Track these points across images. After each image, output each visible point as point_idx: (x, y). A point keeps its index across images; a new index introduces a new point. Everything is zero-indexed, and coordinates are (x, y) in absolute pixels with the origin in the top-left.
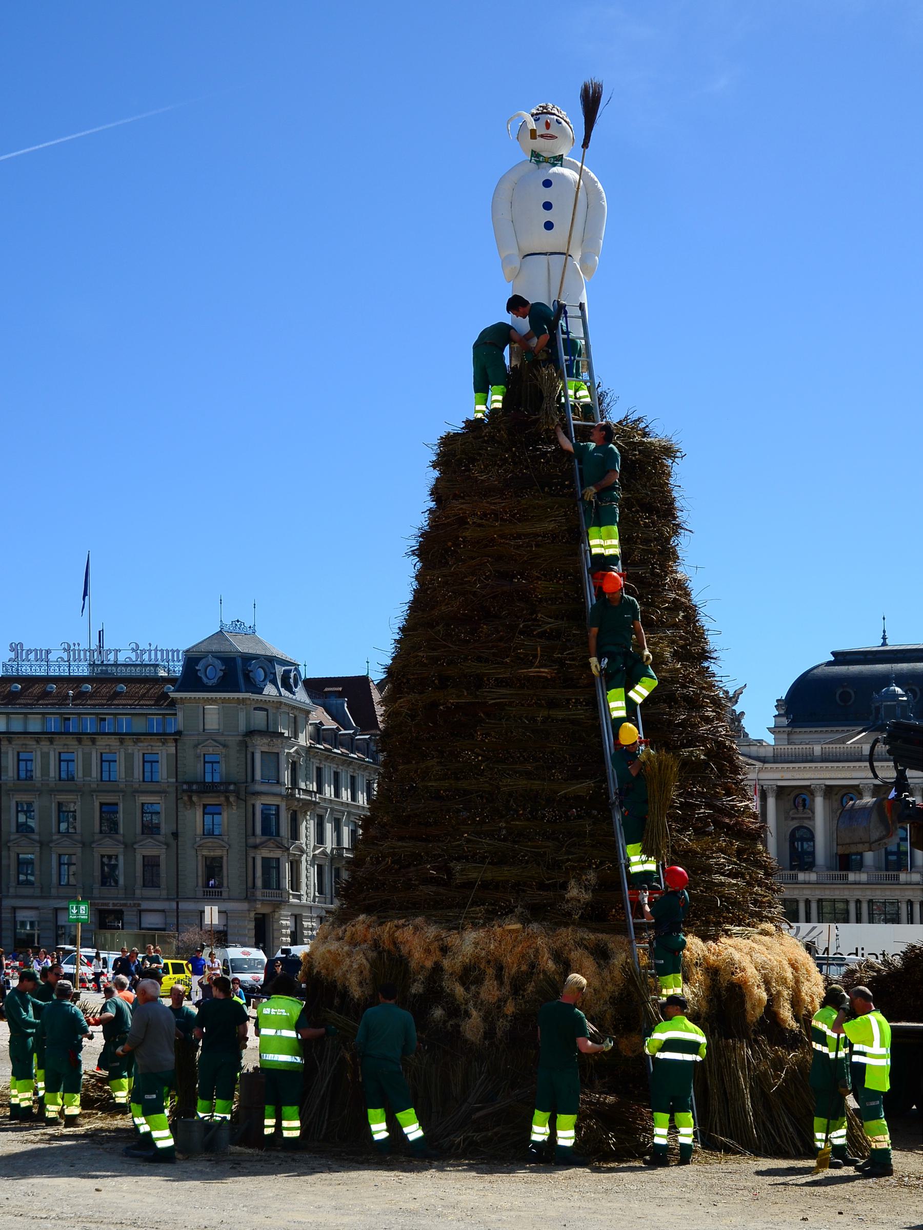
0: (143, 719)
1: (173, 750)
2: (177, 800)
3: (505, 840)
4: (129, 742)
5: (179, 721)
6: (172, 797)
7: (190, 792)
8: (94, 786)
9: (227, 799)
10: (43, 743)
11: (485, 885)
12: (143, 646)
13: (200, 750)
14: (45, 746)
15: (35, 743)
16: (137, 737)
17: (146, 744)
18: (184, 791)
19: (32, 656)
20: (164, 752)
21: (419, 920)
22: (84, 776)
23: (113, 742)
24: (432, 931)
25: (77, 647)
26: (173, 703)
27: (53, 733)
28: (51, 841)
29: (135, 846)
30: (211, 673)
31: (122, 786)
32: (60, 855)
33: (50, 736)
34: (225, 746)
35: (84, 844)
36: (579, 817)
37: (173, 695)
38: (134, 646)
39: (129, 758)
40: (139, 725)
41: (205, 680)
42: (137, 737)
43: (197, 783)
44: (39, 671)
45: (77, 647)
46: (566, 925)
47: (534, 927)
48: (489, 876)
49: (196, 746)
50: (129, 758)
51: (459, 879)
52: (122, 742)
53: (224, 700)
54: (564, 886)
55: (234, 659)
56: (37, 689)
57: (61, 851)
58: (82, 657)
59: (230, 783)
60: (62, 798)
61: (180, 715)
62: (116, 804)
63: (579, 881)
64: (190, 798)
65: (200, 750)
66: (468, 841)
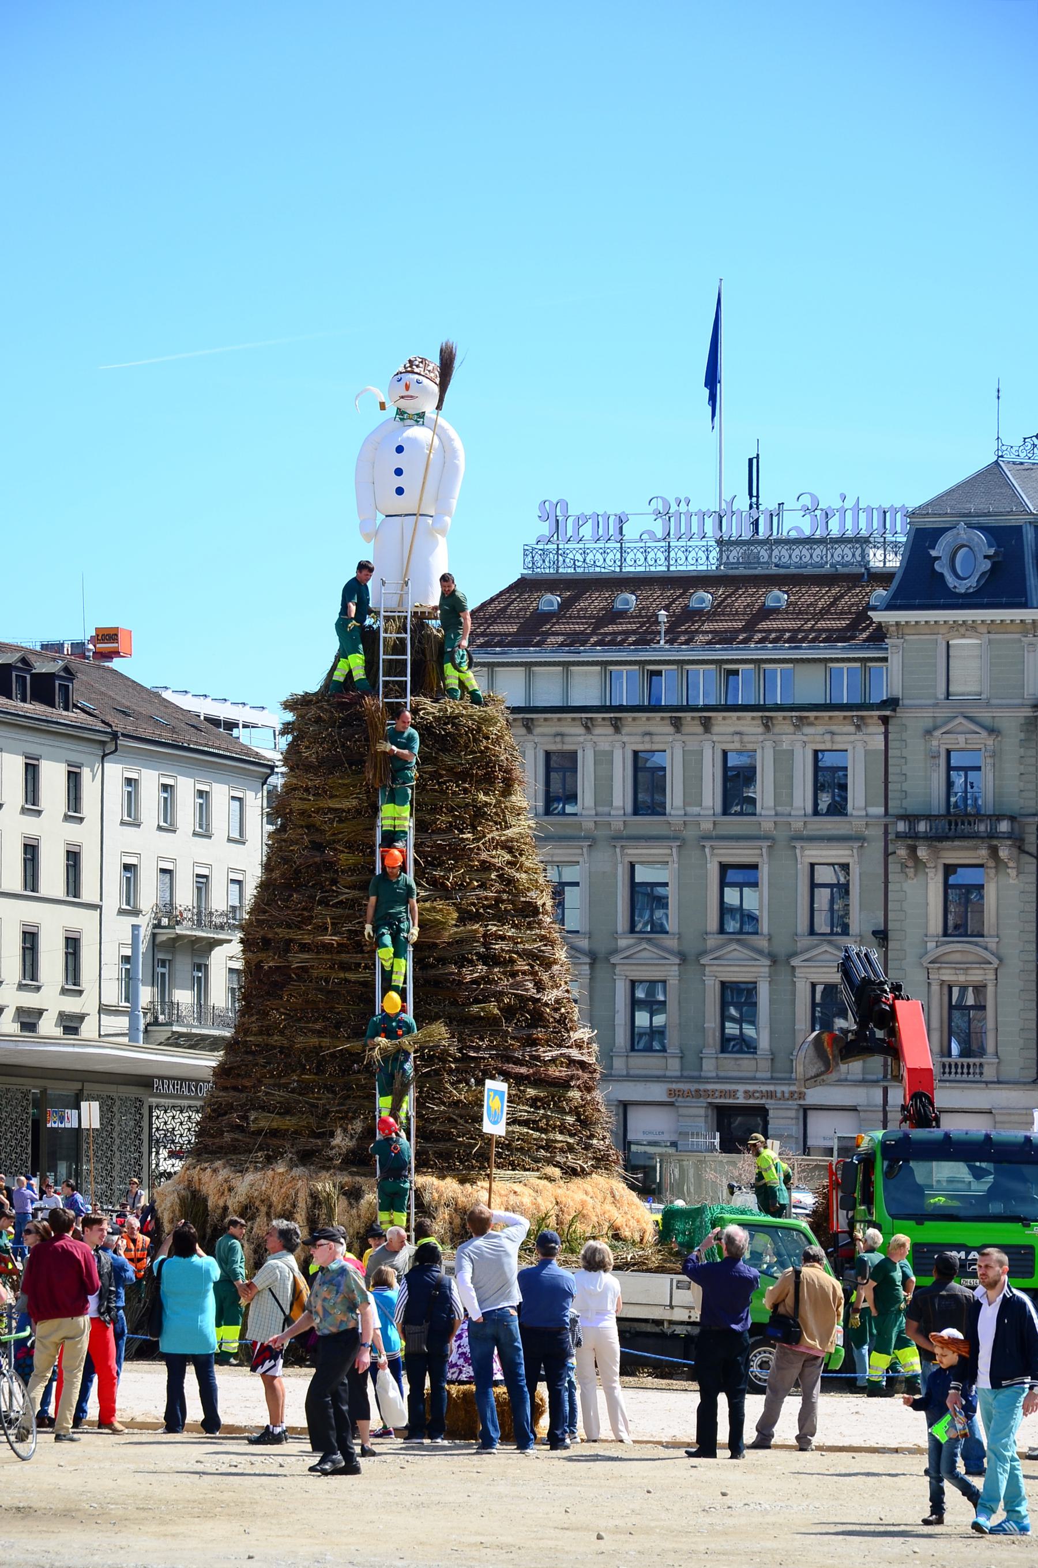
0: (819, 670)
1: (878, 743)
2: (887, 854)
3: (293, 1091)
4: (782, 723)
5: (892, 678)
6: (876, 849)
7: (912, 838)
8: (707, 826)
9: (994, 851)
10: (597, 731)
11: (274, 1133)
12: (829, 501)
13: (940, 742)
14: (603, 735)
15: (581, 730)
16: (801, 712)
17: (820, 729)
18: (899, 836)
19: (587, 531)
20: (858, 748)
21: (218, 1164)
22: (685, 804)
23: (749, 724)
24: (224, 1173)
25: (683, 508)
26: (879, 635)
27: (621, 709)
28: (615, 951)
29: (794, 962)
30: (966, 562)
31: (767, 826)
32: (633, 983)
33: (614, 713)
34: (992, 731)
35: (683, 958)
36: (359, 1071)
37: (877, 616)
38: (806, 500)
39: (784, 760)
40: (809, 686)
41: (951, 581)
42: (801, 712)
43: (928, 817)
44: (604, 562)
45: (683, 508)
46: (328, 1169)
47: (298, 1171)
48: (275, 1125)
49: (929, 732)
50: (784, 760)
51: (253, 1127)
52: (767, 725)
53: (992, 626)
54: (332, 1135)
55: (1018, 529)
56: (594, 603)
57: (637, 974)
58: (694, 529)
59: (999, 817)
60: (634, 852)
61: (895, 661)
62: (755, 867)
63: (345, 1130)
64: (913, 850)
65: (940, 742)
66: (267, 1094)
